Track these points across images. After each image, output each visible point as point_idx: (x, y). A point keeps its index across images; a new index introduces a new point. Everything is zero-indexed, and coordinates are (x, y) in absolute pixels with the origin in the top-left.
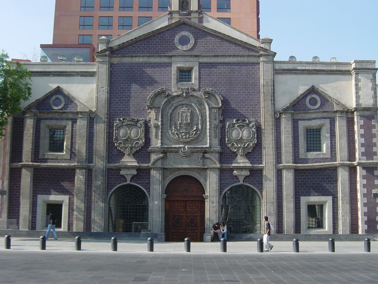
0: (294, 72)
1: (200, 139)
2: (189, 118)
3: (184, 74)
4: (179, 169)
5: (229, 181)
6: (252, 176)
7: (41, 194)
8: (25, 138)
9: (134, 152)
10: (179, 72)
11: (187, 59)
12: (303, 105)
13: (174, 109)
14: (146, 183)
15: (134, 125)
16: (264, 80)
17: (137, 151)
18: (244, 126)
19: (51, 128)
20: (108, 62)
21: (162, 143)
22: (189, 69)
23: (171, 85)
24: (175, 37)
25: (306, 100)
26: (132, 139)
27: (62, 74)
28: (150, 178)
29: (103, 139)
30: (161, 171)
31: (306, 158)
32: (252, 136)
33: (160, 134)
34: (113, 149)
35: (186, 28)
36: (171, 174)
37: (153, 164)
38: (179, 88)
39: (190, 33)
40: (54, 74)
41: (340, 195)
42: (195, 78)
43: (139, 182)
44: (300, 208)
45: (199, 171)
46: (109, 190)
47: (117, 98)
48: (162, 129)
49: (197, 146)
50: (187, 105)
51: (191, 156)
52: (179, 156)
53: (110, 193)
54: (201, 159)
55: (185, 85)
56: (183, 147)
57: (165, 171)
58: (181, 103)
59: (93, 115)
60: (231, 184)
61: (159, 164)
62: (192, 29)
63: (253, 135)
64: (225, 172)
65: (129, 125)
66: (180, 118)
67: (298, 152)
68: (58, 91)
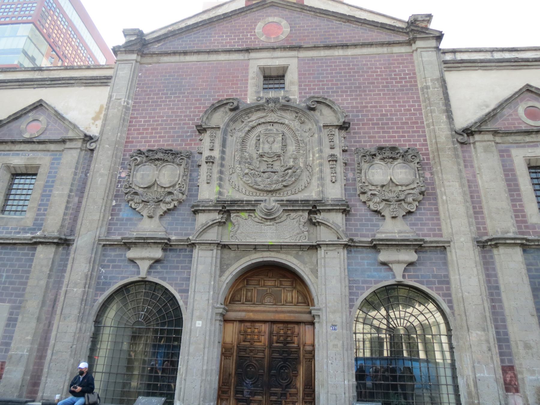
3: (271, 82)
4: (256, 248)
11: (278, 54)
12: (513, 119)
13: (249, 131)
14: (183, 279)
18: (394, 159)
19: (14, 172)
20: (134, 62)
22: (281, 73)
23: (246, 95)
25: (516, 111)
28: (190, 268)
30: (215, 251)
34: (122, 207)
36: (238, 259)
38: (261, 98)
39: (283, 18)
43: (165, 275)
45: (300, 253)
46: (99, 293)
51: (282, 219)
52: (256, 219)
55: (272, 94)
57: (226, 251)
58: (263, 120)
59: (92, 144)
60: (375, 284)
64: (359, 256)
65: (158, 160)
68: (39, 105)
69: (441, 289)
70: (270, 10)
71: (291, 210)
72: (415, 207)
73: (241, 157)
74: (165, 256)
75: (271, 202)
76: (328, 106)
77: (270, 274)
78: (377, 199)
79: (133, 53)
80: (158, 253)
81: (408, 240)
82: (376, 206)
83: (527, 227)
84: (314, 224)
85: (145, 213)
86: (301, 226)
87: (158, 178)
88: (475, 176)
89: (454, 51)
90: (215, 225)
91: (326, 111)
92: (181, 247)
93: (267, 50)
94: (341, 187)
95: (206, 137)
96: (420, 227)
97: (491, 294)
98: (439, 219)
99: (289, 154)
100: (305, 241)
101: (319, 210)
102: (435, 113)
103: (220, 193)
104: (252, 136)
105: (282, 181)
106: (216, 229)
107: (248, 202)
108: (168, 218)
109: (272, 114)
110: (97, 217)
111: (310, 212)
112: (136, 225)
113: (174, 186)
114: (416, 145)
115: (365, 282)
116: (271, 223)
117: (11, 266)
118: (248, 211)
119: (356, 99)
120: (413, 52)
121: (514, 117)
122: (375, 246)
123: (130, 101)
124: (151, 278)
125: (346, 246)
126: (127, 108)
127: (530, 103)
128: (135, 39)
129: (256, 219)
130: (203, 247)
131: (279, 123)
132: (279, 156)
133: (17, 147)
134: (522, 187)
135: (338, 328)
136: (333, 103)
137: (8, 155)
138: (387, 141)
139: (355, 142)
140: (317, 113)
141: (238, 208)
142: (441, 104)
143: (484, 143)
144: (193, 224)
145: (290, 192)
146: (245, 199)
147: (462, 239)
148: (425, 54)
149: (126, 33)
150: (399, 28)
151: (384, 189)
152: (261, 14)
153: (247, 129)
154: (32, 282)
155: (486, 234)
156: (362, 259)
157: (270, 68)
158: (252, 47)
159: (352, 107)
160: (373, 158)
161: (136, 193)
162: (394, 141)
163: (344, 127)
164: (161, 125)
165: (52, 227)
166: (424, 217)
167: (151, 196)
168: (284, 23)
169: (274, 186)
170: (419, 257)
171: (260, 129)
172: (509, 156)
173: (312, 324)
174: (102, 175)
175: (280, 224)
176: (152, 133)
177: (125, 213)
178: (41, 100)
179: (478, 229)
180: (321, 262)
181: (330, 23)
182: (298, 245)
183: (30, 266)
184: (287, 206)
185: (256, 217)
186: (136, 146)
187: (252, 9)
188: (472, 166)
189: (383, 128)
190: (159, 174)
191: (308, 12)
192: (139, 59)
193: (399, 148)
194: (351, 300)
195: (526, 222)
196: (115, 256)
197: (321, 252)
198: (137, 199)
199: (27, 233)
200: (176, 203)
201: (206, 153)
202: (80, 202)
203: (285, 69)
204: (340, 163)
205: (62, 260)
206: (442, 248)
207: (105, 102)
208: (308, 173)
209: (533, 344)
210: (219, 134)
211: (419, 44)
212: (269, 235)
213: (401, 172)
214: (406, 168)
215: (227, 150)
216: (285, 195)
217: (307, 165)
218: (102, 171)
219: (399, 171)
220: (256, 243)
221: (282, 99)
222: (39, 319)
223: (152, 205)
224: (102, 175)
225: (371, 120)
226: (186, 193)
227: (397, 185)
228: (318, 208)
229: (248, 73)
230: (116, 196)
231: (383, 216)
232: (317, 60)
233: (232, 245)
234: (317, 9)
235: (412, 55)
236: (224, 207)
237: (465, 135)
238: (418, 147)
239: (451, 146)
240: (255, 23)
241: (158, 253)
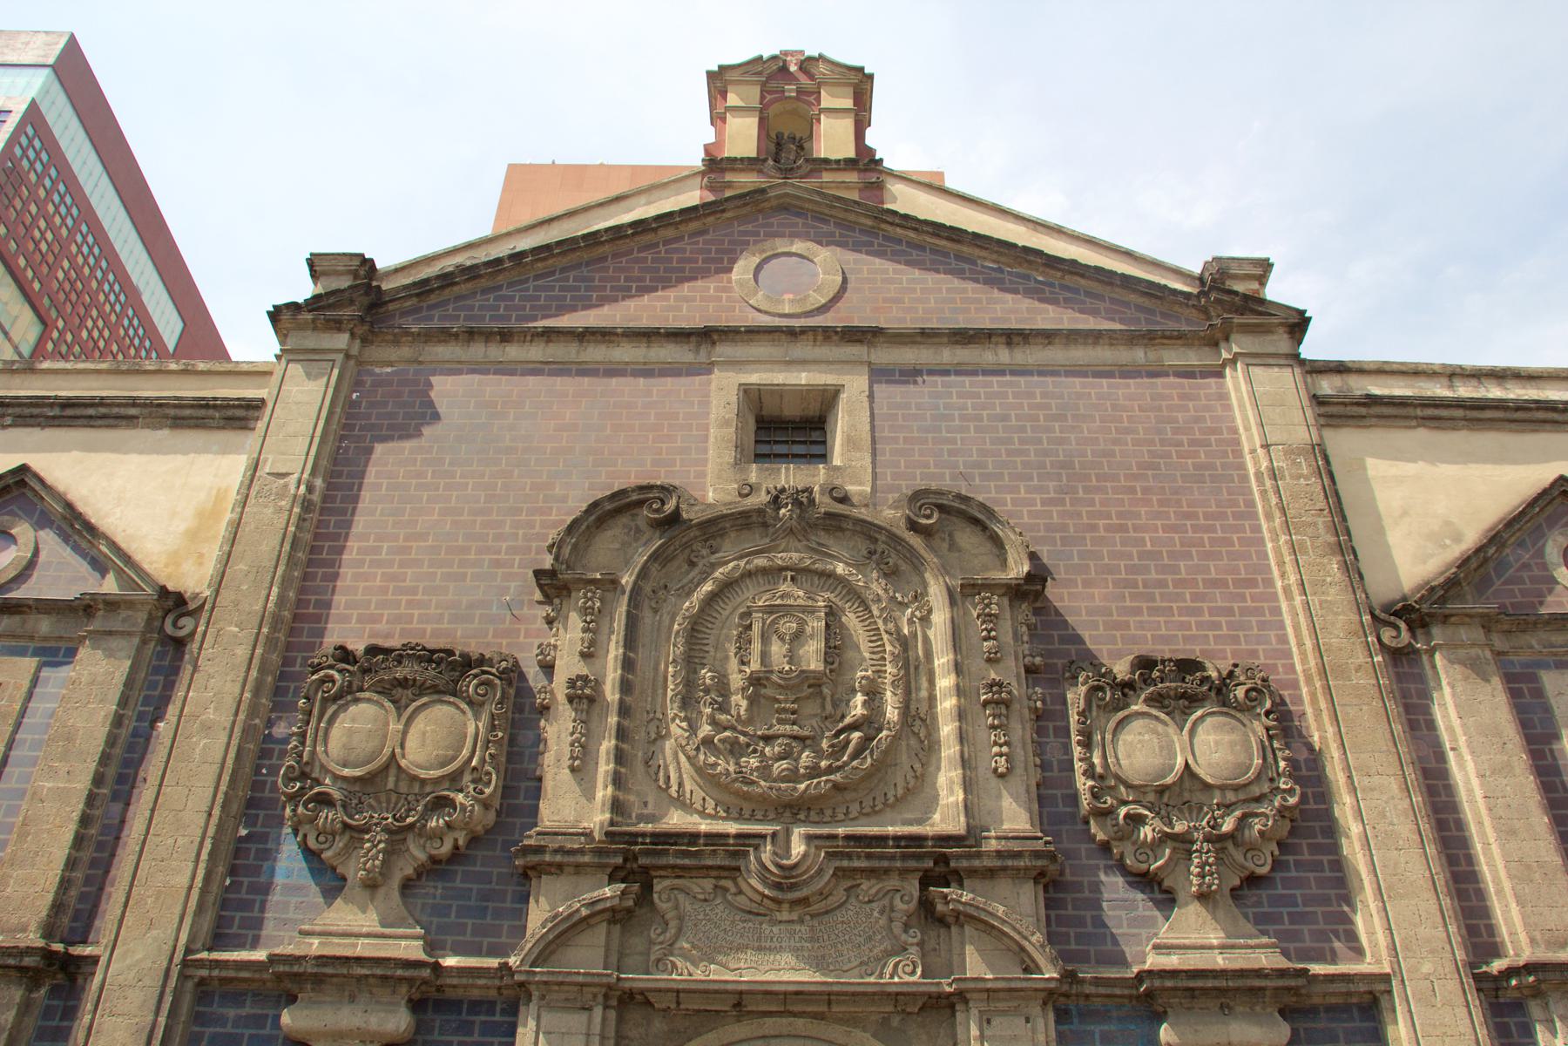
1: (899, 778)
9: (409, 871)
10: (752, 425)
11: (801, 350)
15: (434, 689)
16: (1266, 446)
17: (434, 860)
18: (1193, 700)
20: (340, 357)
21: (617, 806)
22: (813, 410)
23: (703, 475)
25: (1540, 553)
26: (414, 778)
27: (70, 412)
29: (216, 768)
30: (598, 1012)
32: (1257, 761)
33: (607, 745)
37: (549, 949)
40: (27, 411)
42: (851, 442)
48: (624, 710)
49: (874, 830)
50: (799, 573)
51: (832, 901)
52: (741, 899)
54: (906, 927)
55: (789, 476)
56: (774, 835)
57: (635, 1015)
58: (761, 562)
59: (183, 621)
61: (587, 959)
63: (1264, 759)
65: (403, 683)
66: (756, 646)
71: (863, 870)
72: (1269, 861)
74: (420, 1027)
76: (976, 521)
79: (339, 330)
82: (1142, 858)
84: (942, 921)
86: (897, 927)
87: (402, 746)
89: (1340, 368)
90: (598, 918)
92: (475, 994)
93: (766, 337)
94: (1028, 791)
96: (1287, 926)
101: (956, 872)
102: (1306, 553)
104: (726, 613)
106: (599, 935)
107: (715, 838)
108: (434, 890)
109: (794, 543)
111: (926, 881)
114: (1254, 653)
116: (795, 916)
118: (714, 873)
119: (1062, 502)
120: (1223, 366)
121: (1536, 572)
123: (319, 482)
126: (307, 506)
128: (350, 287)
129: (741, 900)
131: (816, 572)
136: (991, 513)
138: (1166, 640)
141: (679, 862)
142: (1320, 526)
145: (854, 809)
147: (1426, 968)
149: (317, 265)
150: (1175, 292)
151: (1165, 799)
152: (750, 227)
157: (779, 392)
158: (723, 321)
159: (1049, 528)
160: (1125, 695)
162: (1186, 639)
166: (1298, 892)
169: (802, 786)
170: (1295, 1032)
172: (1539, 693)
175: (826, 918)
176: (384, 590)
181: (967, 266)
182: (889, 994)
184: (849, 856)
185: (740, 892)
187: (723, 211)
190: (405, 733)
191: (898, 230)
192: (356, 348)
193: (1208, 665)
196: (238, 1021)
198: (327, 816)
201: (568, 666)
203: (829, 397)
204: (1021, 711)
208: (913, 742)
213: (1216, 743)
214: (1233, 729)
216: (841, 817)
218: (210, 714)
219: (1211, 738)
220: (744, 987)
221: (822, 492)
225: (1111, 570)
227: (1207, 787)
228: (953, 864)
231: (1168, 891)
233: (660, 990)
234: (926, 222)
236: (629, 857)
237: (1403, 625)
238: (1262, 660)
239: (1361, 658)
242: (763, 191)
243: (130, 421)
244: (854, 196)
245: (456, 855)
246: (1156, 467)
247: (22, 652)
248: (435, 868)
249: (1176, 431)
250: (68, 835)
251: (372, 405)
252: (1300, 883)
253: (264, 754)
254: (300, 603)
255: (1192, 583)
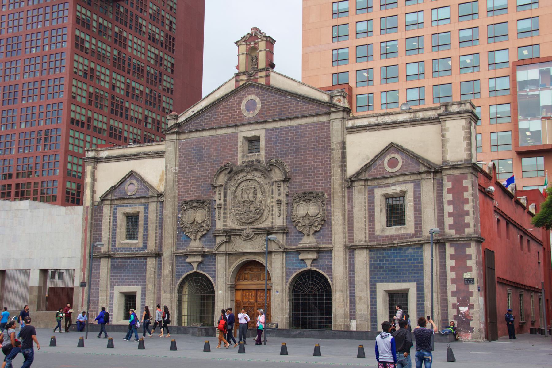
0: (370, 128)
2: (251, 195)
4: (244, 254)
5: (296, 266)
6: (320, 259)
7: (118, 285)
8: (103, 227)
10: (247, 143)
13: (238, 186)
18: (310, 200)
22: (257, 139)
23: (237, 159)
24: (241, 103)
25: (383, 161)
31: (383, 234)
35: (252, 91)
36: (236, 259)
38: (245, 162)
39: (257, 95)
41: (427, 281)
44: (376, 298)
47: (186, 178)
53: (179, 282)
57: (231, 256)
58: (244, 179)
62: (259, 90)
64: (292, 256)
65: (195, 207)
67: (374, 228)
68: (131, 174)
69: (329, 272)
70: (250, 89)
73: (234, 203)
75: (248, 229)
77: (251, 267)
78: (300, 225)
80: (200, 259)
81: (311, 248)
83: (374, 237)
85: (192, 237)
88: (352, 208)
91: (277, 171)
95: (217, 189)
97: (350, 274)
98: (331, 234)
99: (258, 200)
100: (264, 250)
103: (225, 225)
105: (254, 217)
106: (224, 245)
107: (238, 230)
108: (203, 239)
110: (170, 241)
112: (189, 244)
113: (204, 222)
115: (294, 269)
117: (138, 268)
119: (296, 158)
122: (298, 251)
123: (177, 168)
124: (199, 271)
125: (283, 252)
126: (175, 173)
127: (393, 155)
130: (220, 255)
132: (252, 202)
133: (126, 202)
134: (376, 214)
135: (279, 292)
137: (123, 206)
138: (310, 187)
139: (294, 188)
140: (273, 172)
143: (359, 187)
144: (215, 242)
146: (237, 228)
148: (334, 123)
152: (244, 93)
153: (237, 185)
154: (148, 276)
155: (353, 242)
156: (293, 257)
159: (294, 164)
161: (186, 227)
163: (287, 180)
164: (195, 183)
165: (152, 246)
167: (194, 228)
168: (258, 100)
171: (243, 184)
172: (373, 193)
173: (269, 290)
174: (170, 217)
176: (190, 188)
177: (183, 238)
178: (131, 171)
179: (349, 239)
180: (273, 260)
183: (146, 268)
186: (183, 197)
188: (352, 202)
189: (309, 178)
194: (287, 279)
195: (374, 234)
197: (273, 255)
199: (140, 251)
200: (206, 231)
201: (218, 202)
202: (162, 233)
204: (284, 203)
205: (159, 264)
206: (330, 251)
207: (164, 169)
209: (363, 297)
210: (223, 188)
211: (333, 116)
212: (248, 247)
215: (228, 199)
217: (265, 205)
222: (154, 293)
223: (194, 234)
224: (170, 217)
225: (303, 173)
226: (210, 225)
229: (237, 142)
230: (178, 228)
232: (276, 129)
235: (329, 123)
239: (340, 190)
240: (241, 101)
241: (200, 259)
242: (245, 84)
243: (145, 158)
244: (262, 81)
245: (205, 234)
246: (314, 148)
247: (141, 205)
248: (202, 236)
249: (319, 138)
250: (154, 236)
251: (183, 149)
252: (325, 232)
253: (178, 220)
254: (179, 192)
255: (317, 174)
